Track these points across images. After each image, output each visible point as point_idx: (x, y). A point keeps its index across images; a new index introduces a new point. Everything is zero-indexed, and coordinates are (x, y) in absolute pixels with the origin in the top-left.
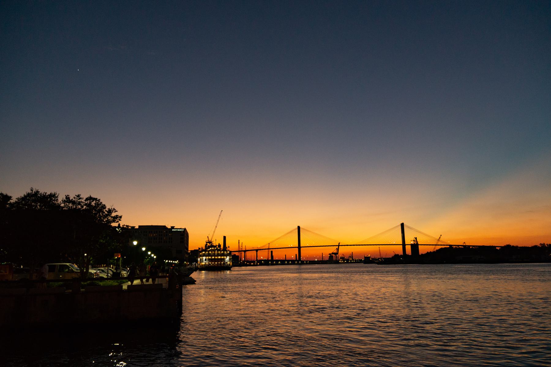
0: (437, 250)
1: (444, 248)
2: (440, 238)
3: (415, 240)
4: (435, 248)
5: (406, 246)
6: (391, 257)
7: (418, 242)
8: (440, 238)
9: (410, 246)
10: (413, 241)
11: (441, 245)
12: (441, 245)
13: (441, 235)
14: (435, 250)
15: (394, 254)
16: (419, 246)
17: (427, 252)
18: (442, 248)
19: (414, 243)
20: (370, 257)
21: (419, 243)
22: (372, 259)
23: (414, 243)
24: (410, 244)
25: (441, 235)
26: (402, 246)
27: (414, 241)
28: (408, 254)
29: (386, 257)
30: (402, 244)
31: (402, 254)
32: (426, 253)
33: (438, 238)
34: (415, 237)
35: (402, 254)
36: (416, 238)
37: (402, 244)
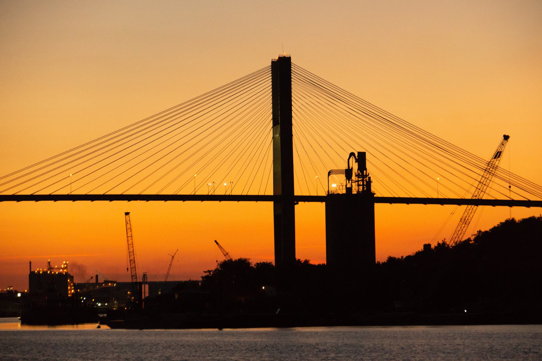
0: (482, 236)
1: (525, 221)
2: (498, 155)
3: (355, 166)
4: (465, 221)
5: (300, 208)
6: (198, 276)
7: (369, 183)
8: (498, 155)
9: (321, 206)
10: (343, 177)
11: (511, 203)
12: (511, 203)
13: (506, 138)
14: (470, 233)
15: (222, 258)
16: (378, 207)
17: (421, 248)
18: (510, 224)
19: (349, 190)
20: (67, 276)
21: (378, 190)
22: (76, 287)
23: (349, 190)
24: (323, 194)
25: (506, 138)
26: (270, 205)
27: (348, 173)
28: (303, 259)
29: (170, 279)
30: (270, 192)
31: (270, 257)
32: (418, 254)
33: (489, 156)
34: (357, 150)
35: (270, 257)
36: (361, 158)
37: (270, 192)
